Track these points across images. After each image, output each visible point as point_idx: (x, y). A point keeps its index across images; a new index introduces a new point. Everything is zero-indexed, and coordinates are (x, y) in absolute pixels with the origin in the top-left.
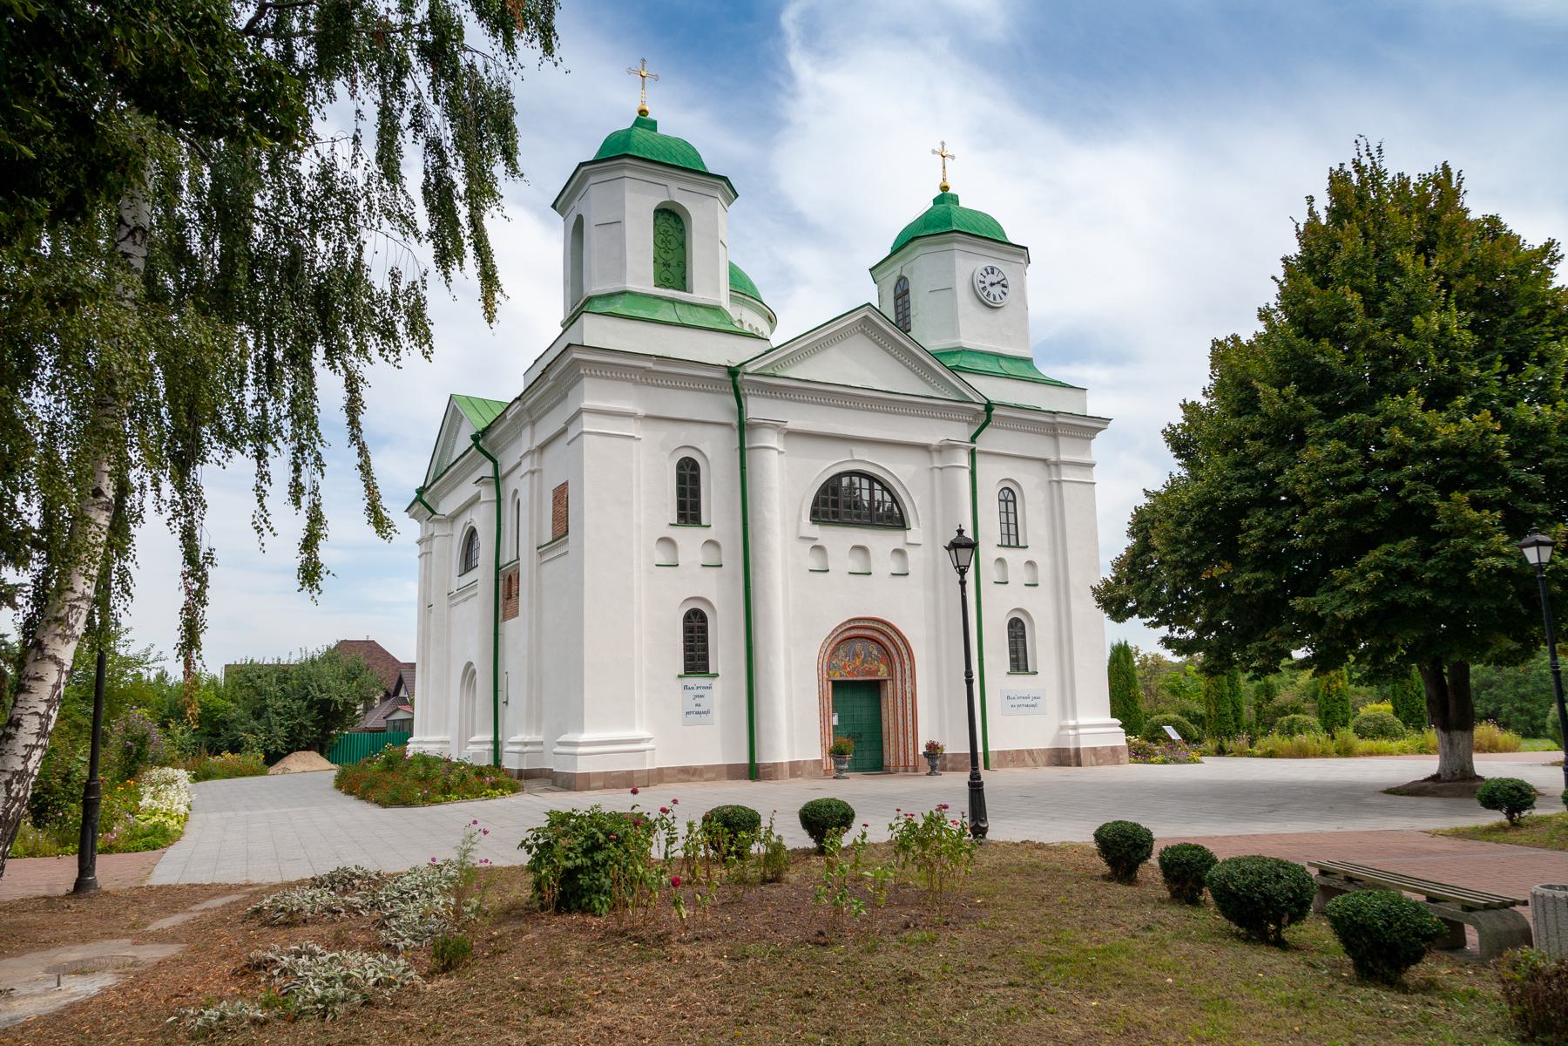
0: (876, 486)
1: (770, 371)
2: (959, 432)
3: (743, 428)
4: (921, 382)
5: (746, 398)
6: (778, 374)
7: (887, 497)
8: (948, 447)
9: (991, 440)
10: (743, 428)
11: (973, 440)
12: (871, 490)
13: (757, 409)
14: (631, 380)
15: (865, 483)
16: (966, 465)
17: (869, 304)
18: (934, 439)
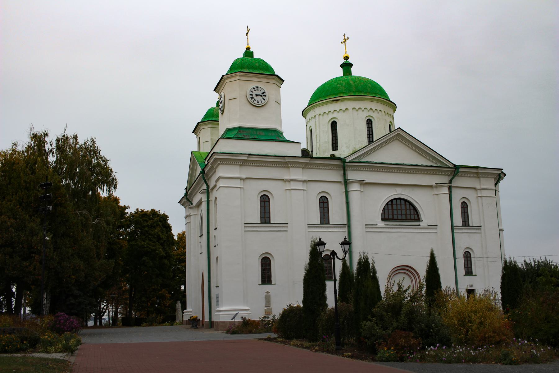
0: (407, 203)
1: (357, 160)
2: (445, 180)
3: (346, 183)
4: (425, 159)
5: (347, 170)
6: (363, 160)
7: (412, 208)
8: (439, 185)
9: (458, 182)
10: (346, 183)
11: (450, 182)
12: (405, 205)
13: (351, 175)
14: (301, 167)
15: (403, 202)
16: (448, 193)
17: (399, 128)
18: (434, 184)
